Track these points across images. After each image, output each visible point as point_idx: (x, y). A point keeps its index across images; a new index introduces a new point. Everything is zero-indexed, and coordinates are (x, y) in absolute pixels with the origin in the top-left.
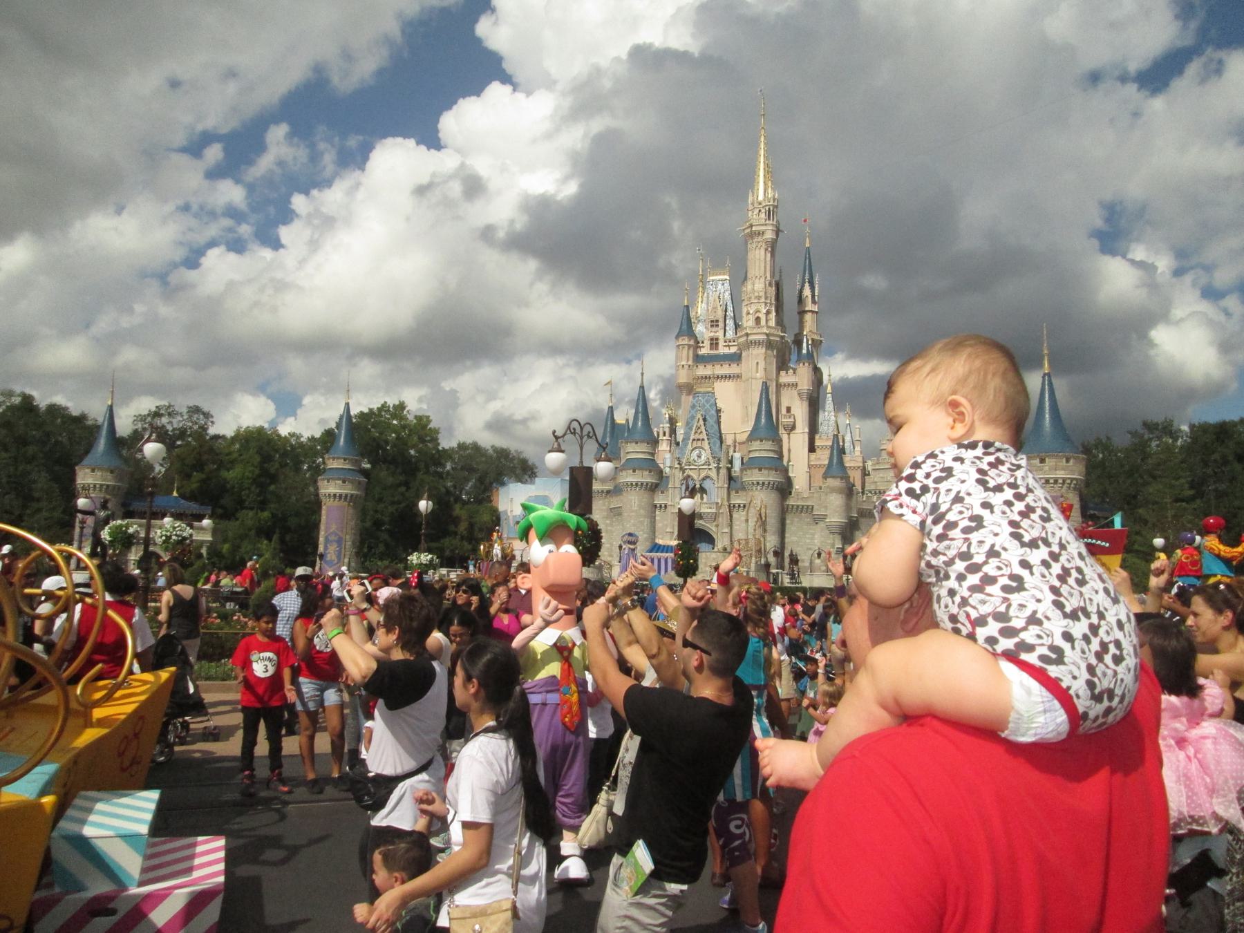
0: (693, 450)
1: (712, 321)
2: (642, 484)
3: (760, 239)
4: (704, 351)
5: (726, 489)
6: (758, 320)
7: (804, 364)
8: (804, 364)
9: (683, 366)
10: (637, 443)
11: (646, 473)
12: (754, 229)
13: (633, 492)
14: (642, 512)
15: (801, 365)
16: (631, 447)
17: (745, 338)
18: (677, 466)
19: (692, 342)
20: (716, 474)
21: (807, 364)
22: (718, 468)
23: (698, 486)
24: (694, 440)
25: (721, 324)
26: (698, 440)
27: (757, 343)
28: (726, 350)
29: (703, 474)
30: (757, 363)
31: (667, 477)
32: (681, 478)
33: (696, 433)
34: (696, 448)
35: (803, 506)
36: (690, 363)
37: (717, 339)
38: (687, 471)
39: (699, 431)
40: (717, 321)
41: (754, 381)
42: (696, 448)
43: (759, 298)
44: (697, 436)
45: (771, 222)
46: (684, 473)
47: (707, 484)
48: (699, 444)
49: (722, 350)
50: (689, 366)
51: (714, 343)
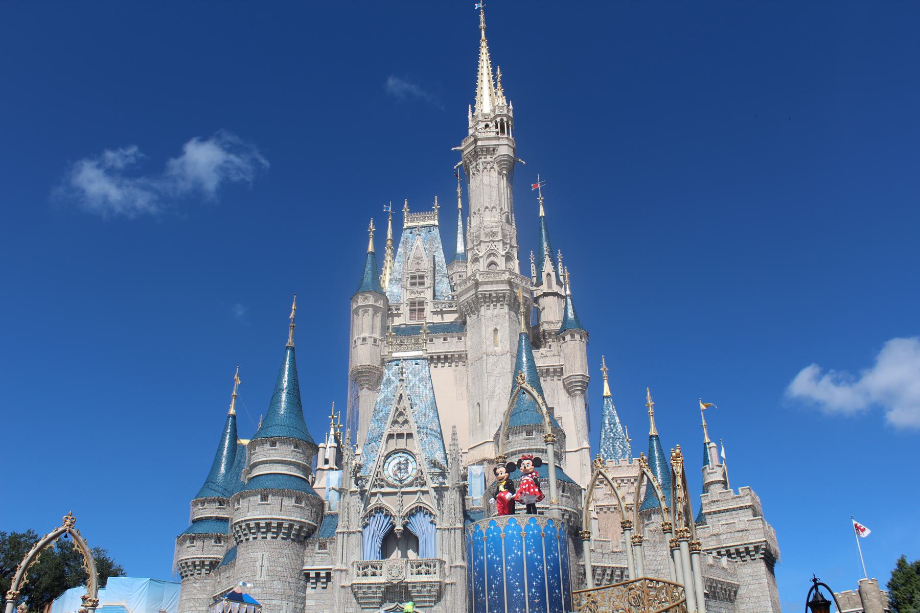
0: (388, 456)
1: (413, 278)
2: (280, 525)
3: (489, 159)
4: (403, 319)
5: (459, 532)
7: (573, 336)
8: (573, 336)
9: (364, 339)
10: (273, 444)
11: (289, 502)
12: (479, 143)
14: (277, 585)
15: (568, 337)
16: (263, 453)
17: (473, 292)
18: (354, 488)
19: (380, 304)
20: (436, 506)
21: (577, 337)
22: (440, 490)
23: (399, 527)
24: (391, 436)
25: (428, 282)
27: (493, 299)
29: (410, 502)
30: (496, 330)
31: (335, 516)
32: (362, 514)
33: (395, 422)
34: (396, 452)
35: (613, 570)
36: (377, 335)
37: (422, 303)
38: (373, 501)
39: (401, 419)
40: (422, 277)
41: (490, 358)
42: (396, 452)
43: (493, 234)
44: (397, 429)
45: (506, 136)
46: (367, 503)
47: (420, 525)
48: (401, 444)
50: (375, 340)
51: (417, 307)
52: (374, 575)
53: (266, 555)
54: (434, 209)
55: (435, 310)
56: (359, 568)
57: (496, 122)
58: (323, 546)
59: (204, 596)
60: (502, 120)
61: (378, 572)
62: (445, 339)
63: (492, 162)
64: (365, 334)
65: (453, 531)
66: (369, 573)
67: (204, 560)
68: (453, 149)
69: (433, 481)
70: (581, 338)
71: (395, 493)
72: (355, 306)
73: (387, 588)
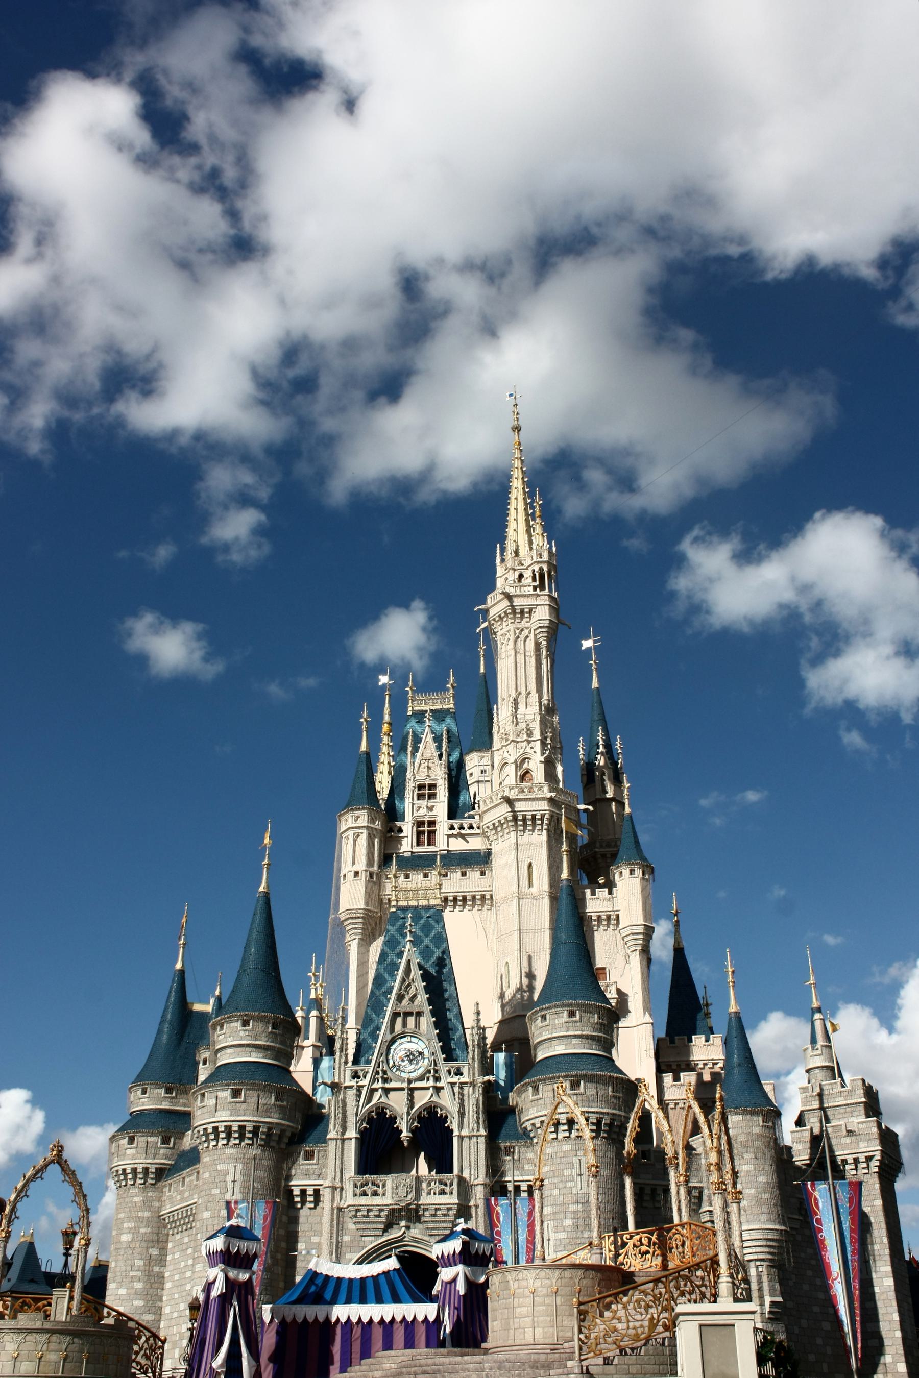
0: (393, 1041)
5: (482, 1141)
6: (524, 776)
7: (632, 872)
9: (356, 874)
13: (229, 1151)
15: (626, 872)
24: (395, 1015)
26: (407, 1014)
28: (457, 845)
30: (530, 865)
33: (400, 998)
34: (402, 1035)
37: (432, 823)
40: (433, 786)
49: (442, 843)
50: (371, 875)
52: (375, 1194)
53: (240, 1166)
54: (448, 689)
55: (450, 832)
56: (356, 1186)
57: (534, 571)
58: (309, 1156)
59: (147, 1214)
60: (541, 569)
61: (380, 1191)
62: (464, 874)
63: (527, 628)
64: (356, 868)
65: (474, 1139)
66: (369, 1192)
67: (149, 1166)
68: (476, 609)
69: (450, 1074)
70: (644, 874)
71: (402, 1089)
72: (343, 828)
73: (392, 1211)
